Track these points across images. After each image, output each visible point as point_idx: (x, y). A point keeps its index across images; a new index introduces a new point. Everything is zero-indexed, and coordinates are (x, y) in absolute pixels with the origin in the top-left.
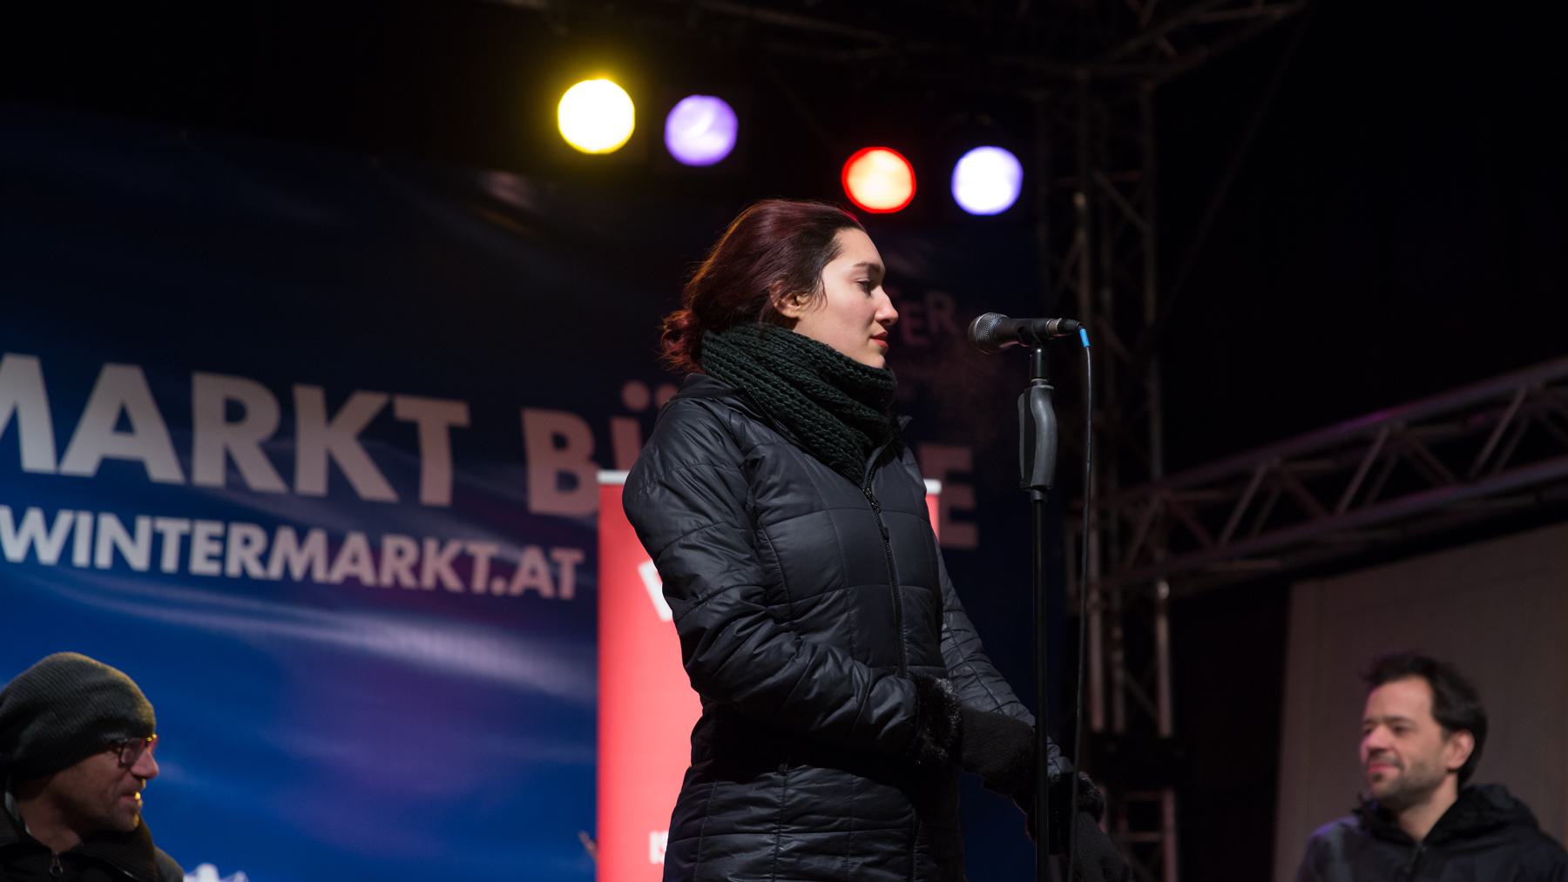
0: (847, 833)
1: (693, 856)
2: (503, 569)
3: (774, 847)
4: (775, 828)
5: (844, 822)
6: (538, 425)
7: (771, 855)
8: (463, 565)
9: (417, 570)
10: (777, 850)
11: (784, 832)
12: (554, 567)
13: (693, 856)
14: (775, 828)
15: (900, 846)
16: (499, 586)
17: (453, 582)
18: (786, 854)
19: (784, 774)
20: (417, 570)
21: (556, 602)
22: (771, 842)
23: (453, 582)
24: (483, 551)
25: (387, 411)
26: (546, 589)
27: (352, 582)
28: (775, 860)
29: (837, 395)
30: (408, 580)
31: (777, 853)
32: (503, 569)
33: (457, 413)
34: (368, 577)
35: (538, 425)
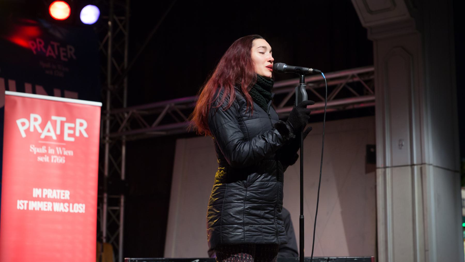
0: (261, 204)
1: (220, 209)
3: (243, 207)
4: (244, 202)
5: (261, 201)
7: (243, 209)
10: (244, 208)
11: (246, 203)
13: (220, 209)
14: (244, 202)
15: (273, 208)
18: (247, 209)
19: (246, 188)
22: (243, 205)
28: (244, 210)
29: (260, 88)
31: (244, 209)
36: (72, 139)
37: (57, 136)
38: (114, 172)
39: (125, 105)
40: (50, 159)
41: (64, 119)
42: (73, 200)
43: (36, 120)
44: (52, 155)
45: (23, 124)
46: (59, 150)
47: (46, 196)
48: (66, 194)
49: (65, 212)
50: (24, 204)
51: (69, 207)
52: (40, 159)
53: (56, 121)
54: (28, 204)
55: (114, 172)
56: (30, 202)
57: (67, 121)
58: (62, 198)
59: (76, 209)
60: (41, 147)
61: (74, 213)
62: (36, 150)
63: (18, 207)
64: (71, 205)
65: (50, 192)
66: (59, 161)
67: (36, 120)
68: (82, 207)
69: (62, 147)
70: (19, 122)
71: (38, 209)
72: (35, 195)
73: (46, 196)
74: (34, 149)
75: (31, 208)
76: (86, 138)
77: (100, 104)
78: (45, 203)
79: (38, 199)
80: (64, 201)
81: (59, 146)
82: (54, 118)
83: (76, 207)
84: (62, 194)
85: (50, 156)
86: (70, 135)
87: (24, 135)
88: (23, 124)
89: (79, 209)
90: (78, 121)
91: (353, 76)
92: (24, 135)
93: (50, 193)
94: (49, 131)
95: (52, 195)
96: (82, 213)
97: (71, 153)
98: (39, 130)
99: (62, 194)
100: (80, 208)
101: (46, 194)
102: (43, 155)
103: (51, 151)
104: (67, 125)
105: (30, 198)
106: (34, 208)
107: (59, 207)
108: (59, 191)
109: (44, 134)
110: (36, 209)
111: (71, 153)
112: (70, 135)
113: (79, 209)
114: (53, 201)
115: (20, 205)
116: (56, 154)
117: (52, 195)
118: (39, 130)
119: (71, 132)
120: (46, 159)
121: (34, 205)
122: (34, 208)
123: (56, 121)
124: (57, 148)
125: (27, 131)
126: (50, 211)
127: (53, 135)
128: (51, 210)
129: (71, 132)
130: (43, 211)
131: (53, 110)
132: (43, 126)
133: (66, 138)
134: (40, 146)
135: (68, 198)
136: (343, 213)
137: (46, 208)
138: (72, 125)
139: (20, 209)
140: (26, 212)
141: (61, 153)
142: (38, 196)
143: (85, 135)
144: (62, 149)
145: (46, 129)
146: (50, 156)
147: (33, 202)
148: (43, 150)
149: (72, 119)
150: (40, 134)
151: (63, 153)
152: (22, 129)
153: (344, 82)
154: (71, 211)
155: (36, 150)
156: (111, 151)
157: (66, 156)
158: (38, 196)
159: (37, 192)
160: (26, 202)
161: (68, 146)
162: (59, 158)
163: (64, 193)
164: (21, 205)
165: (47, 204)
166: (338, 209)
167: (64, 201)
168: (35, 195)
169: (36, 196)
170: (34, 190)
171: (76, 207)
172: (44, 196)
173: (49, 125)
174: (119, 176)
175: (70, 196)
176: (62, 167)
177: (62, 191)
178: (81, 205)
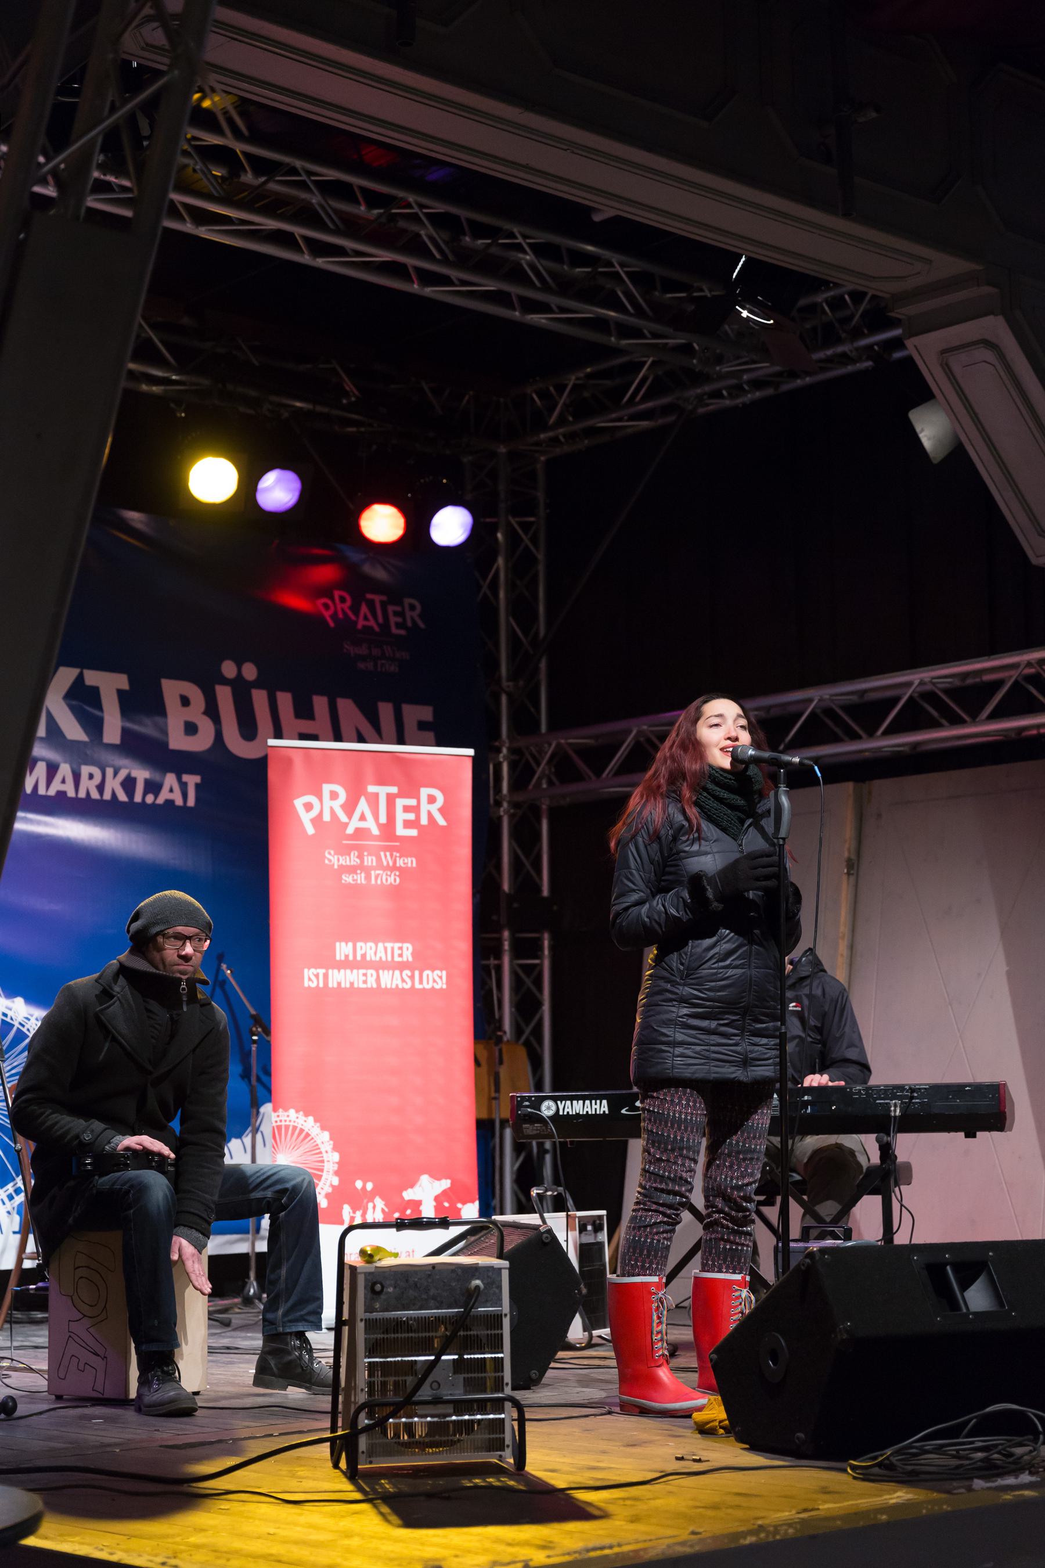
2: (152, 787)
6: (172, 689)
8: (129, 784)
9: (101, 788)
12: (184, 787)
16: (150, 799)
17: (122, 797)
20: (101, 788)
21: (185, 807)
23: (122, 797)
24: (142, 774)
25: (80, 678)
26: (179, 802)
27: (61, 794)
30: (95, 795)
32: (152, 787)
33: (122, 681)
34: (71, 793)
35: (172, 689)
36: (413, 832)
37: (380, 826)
38: (526, 883)
39: (544, 728)
40: (368, 877)
41: (394, 790)
42: (421, 962)
43: (334, 795)
44: (372, 868)
45: (308, 807)
46: (386, 859)
47: (364, 956)
48: (407, 952)
49: (403, 989)
50: (317, 976)
51: (412, 977)
52: (348, 879)
53: (377, 795)
54: (326, 976)
55: (526, 883)
56: (330, 971)
57: (401, 795)
58: (397, 959)
59: (428, 983)
60: (349, 855)
61: (424, 989)
62: (338, 860)
63: (306, 983)
64: (417, 973)
65: (371, 948)
66: (387, 880)
67: (334, 795)
68: (441, 977)
69: (391, 849)
70: (299, 803)
71: (348, 986)
72: (339, 956)
73: (364, 956)
74: (333, 859)
75: (332, 985)
76: (443, 827)
77: (471, 752)
78: (362, 971)
79: (347, 964)
80: (402, 966)
81: (386, 849)
82: (372, 789)
83: (428, 975)
84: (397, 952)
85: (367, 870)
86: (407, 824)
87: (310, 830)
88: (308, 807)
89: (434, 981)
90: (425, 792)
91: (1029, 664)
92: (310, 830)
93: (369, 950)
94: (363, 818)
95: (375, 953)
96: (441, 989)
97: (411, 862)
98: (343, 817)
99: (397, 952)
100: (435, 979)
101: (363, 952)
102: (352, 870)
103: (369, 860)
104: (400, 803)
105: (332, 963)
106: (339, 984)
107: (390, 980)
108: (389, 945)
109: (354, 824)
110: (343, 986)
111: (411, 862)
112: (407, 824)
113: (434, 981)
114: (379, 966)
115: (310, 979)
116: (380, 866)
117: (375, 953)
118: (343, 817)
119: (411, 816)
120: (360, 878)
121: (338, 978)
122: (339, 984)
123: (377, 795)
124: (382, 854)
125: (317, 821)
126: (372, 988)
127: (371, 824)
128: (375, 986)
129: (411, 816)
130: (359, 989)
131: (369, 771)
132: (350, 808)
133: (401, 831)
134: (346, 851)
135: (410, 959)
136: (1009, 975)
137: (365, 982)
138: (412, 802)
139: (309, 987)
140: (322, 993)
141: (391, 864)
142: (347, 956)
143: (441, 821)
144: (391, 856)
145: (357, 814)
146: (367, 870)
147: (336, 971)
148: (353, 859)
149: (410, 789)
150: (346, 825)
151: (395, 862)
152: (306, 818)
153: (1014, 674)
154: (418, 986)
155: (338, 860)
156: (515, 835)
157: (400, 869)
158: (347, 956)
159: (343, 950)
160: (321, 971)
161: (404, 846)
162: (387, 875)
163: (401, 948)
164: (311, 978)
165: (365, 975)
166: (1000, 966)
167: (402, 966)
168: (339, 956)
169: (343, 958)
170: (338, 944)
171: (428, 975)
172: (359, 958)
173: (363, 805)
174: (539, 889)
175: (413, 954)
176: (394, 893)
177: (397, 945)
178: (438, 972)
